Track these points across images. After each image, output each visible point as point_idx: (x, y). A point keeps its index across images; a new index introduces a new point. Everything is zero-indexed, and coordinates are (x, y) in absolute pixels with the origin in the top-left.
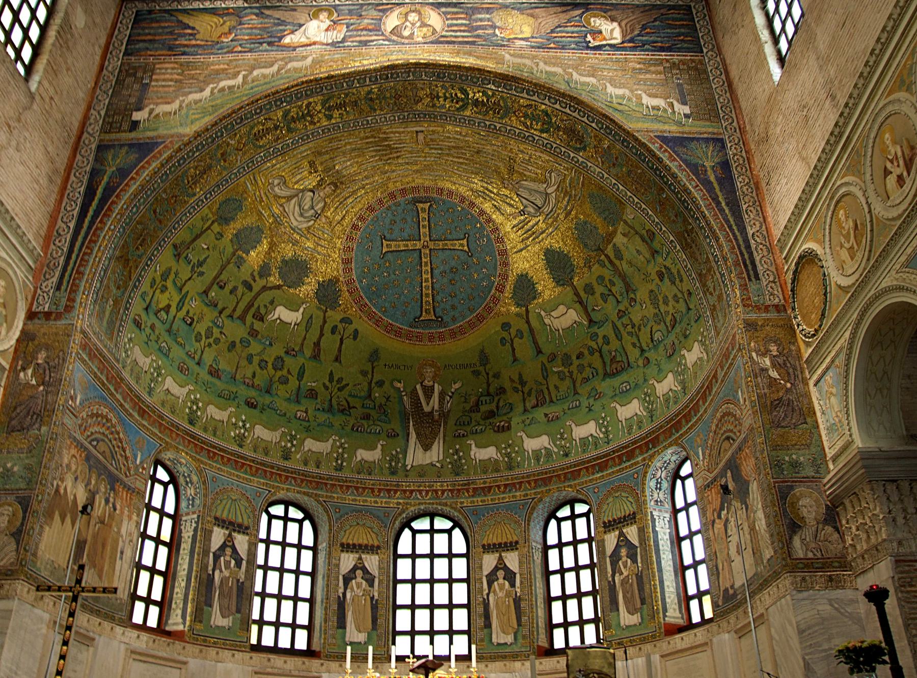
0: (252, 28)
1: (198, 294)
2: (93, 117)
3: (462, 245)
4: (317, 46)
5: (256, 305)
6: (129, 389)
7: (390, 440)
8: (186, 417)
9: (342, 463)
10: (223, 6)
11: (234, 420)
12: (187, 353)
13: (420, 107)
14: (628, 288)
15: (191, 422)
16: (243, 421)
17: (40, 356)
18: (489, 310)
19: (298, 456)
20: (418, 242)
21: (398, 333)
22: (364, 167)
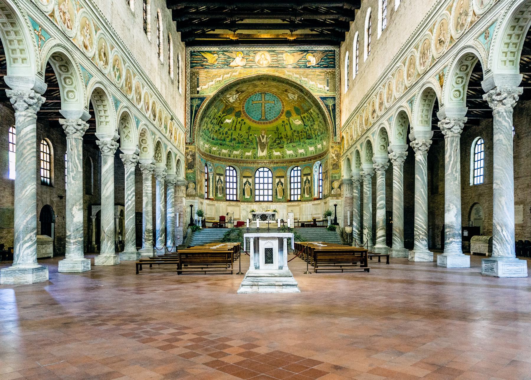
14: (313, 121)
18: (279, 117)
21: (255, 122)
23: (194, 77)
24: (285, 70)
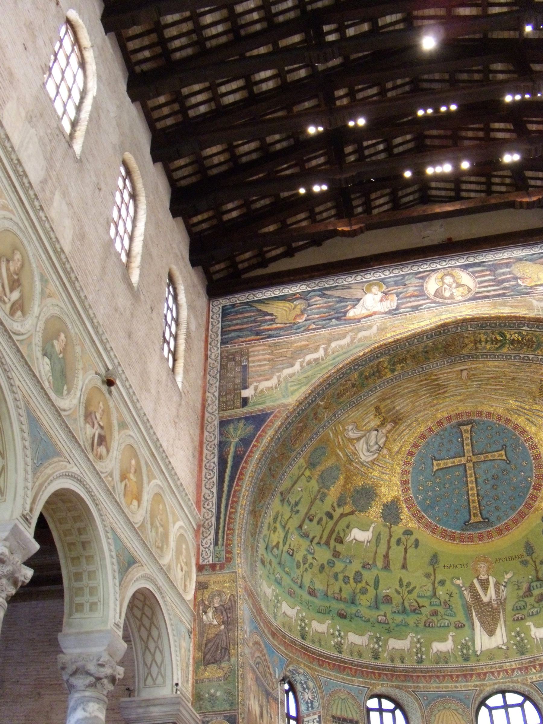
0: (319, 308)
1: (296, 529)
2: (210, 399)
3: (500, 455)
4: (377, 316)
5: (336, 531)
6: (265, 617)
7: (459, 631)
8: (299, 633)
9: (422, 656)
10: (291, 292)
11: (331, 631)
12: (292, 580)
13: (465, 352)
15: (303, 638)
16: (339, 631)
17: (215, 601)
18: (529, 506)
19: (385, 655)
20: (462, 459)
21: (452, 537)
22: (417, 404)
23: (231, 365)
24: (529, 299)
